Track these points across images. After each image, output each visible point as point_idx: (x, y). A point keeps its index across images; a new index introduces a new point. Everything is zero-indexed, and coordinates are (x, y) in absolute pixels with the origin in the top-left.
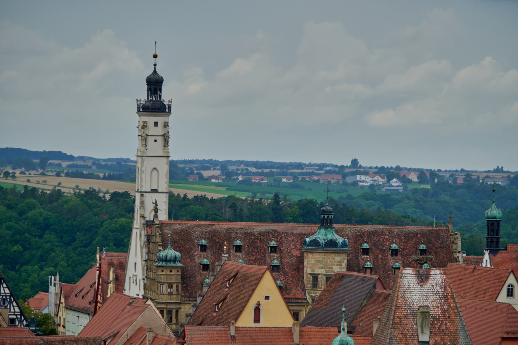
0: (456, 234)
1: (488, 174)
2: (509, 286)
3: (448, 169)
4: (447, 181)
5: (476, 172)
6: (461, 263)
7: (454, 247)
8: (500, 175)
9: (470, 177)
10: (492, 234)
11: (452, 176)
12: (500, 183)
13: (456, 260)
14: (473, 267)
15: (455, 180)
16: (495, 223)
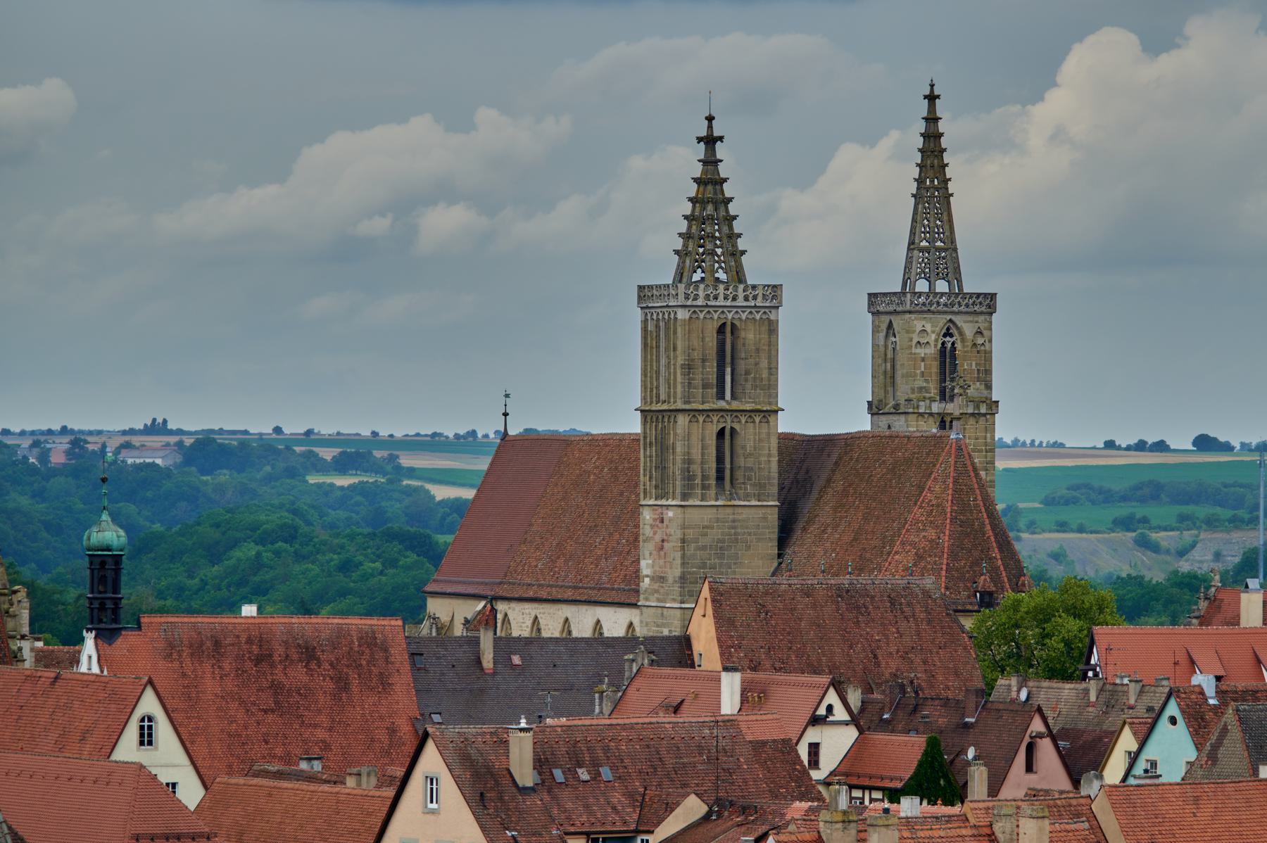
0: (15, 592)
1: (127, 438)
2: (142, 720)
3: (29, 428)
4: (25, 458)
5: (100, 433)
6: (27, 665)
7: (10, 624)
8: (157, 440)
9: (83, 448)
10: (101, 588)
11: (36, 444)
12: (159, 461)
13: (16, 657)
14: (53, 675)
15: (44, 456)
16: (109, 560)
